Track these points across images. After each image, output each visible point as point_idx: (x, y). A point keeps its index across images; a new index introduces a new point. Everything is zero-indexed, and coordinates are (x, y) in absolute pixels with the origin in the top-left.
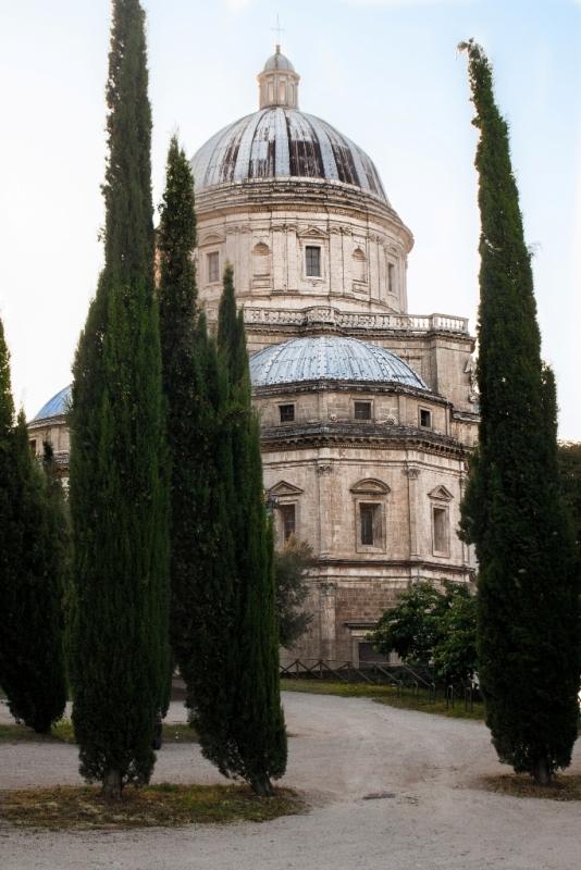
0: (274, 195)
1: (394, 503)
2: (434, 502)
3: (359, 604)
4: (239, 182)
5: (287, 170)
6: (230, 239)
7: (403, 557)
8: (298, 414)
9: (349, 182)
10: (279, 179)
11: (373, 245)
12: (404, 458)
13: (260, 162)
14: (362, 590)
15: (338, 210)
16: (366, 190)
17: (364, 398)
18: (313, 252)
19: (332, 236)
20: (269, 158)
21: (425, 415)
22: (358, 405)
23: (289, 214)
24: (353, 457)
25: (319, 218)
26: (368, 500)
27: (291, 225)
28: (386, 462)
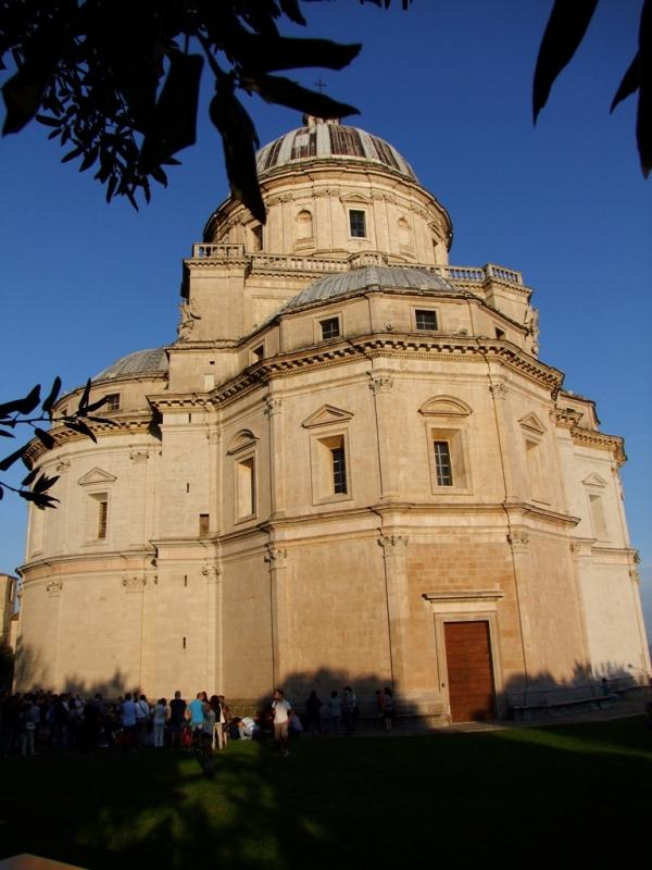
1: (477, 429)
3: (441, 567)
5: (329, 150)
7: (497, 499)
8: (346, 328)
11: (418, 217)
12: (486, 372)
13: (302, 148)
14: (443, 546)
15: (381, 179)
19: (375, 202)
21: (499, 333)
22: (418, 313)
23: (331, 182)
24: (419, 369)
25: (362, 185)
26: (442, 423)
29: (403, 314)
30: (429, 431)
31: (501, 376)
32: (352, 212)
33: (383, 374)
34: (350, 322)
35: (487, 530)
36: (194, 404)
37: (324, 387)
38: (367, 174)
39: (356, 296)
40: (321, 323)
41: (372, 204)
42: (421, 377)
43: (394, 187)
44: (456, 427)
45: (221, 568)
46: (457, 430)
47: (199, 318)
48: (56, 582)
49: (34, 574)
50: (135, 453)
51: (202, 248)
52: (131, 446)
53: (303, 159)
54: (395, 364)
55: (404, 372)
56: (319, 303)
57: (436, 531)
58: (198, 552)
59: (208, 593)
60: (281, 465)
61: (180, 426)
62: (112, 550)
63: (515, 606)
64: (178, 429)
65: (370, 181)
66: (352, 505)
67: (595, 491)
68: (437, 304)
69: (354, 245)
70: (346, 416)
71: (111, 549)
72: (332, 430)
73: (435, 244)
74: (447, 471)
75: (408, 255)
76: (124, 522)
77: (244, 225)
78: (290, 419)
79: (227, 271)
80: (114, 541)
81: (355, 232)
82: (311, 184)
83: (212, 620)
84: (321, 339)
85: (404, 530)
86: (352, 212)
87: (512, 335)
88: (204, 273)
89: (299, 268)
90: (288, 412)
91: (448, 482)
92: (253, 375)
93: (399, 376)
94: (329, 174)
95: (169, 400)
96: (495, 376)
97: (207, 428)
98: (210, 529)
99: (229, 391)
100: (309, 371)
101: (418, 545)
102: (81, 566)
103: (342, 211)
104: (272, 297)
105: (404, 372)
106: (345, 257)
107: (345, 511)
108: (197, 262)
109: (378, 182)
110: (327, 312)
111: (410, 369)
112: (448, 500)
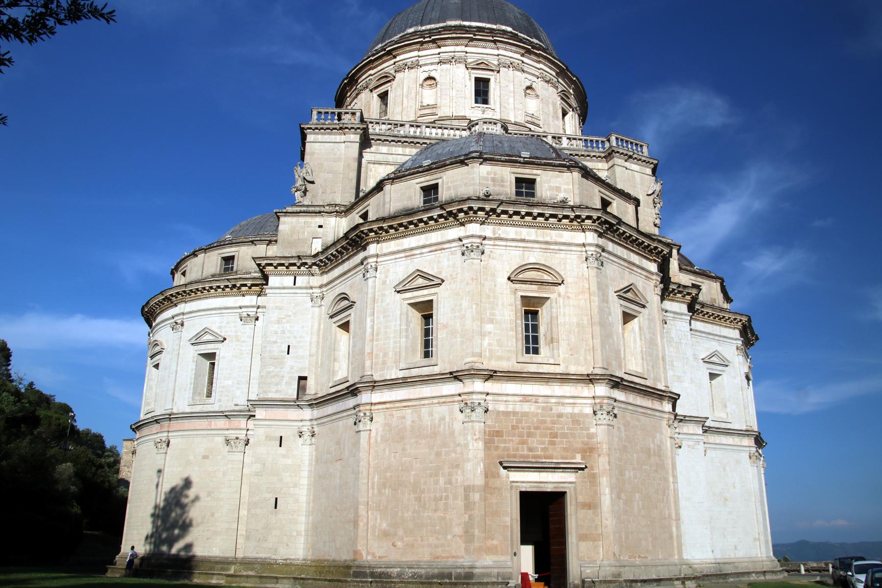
2: (622, 302)
3: (521, 435)
6: (399, 76)
8: (444, 195)
14: (525, 414)
15: (508, 47)
17: (527, 172)
21: (605, 204)
22: (519, 181)
25: (488, 52)
26: (532, 291)
27: (460, 58)
28: (556, 243)
29: (502, 181)
30: (519, 298)
31: (597, 246)
32: (478, 80)
33: (474, 240)
34: (449, 188)
35: (571, 401)
36: (299, 267)
37: (418, 252)
38: (495, 42)
39: (456, 163)
40: (422, 188)
41: (498, 72)
42: (514, 244)
43: (522, 55)
44: (545, 296)
45: (316, 429)
46: (548, 298)
47: (313, 182)
48: (164, 439)
49: (145, 431)
50: (245, 314)
51: (319, 113)
52: (240, 308)
54: (488, 230)
55: (496, 239)
56: (420, 169)
57: (517, 398)
58: (293, 413)
59: (303, 452)
61: (284, 288)
62: (217, 409)
63: (593, 478)
64: (283, 291)
65: (498, 49)
66: (436, 370)
67: (716, 369)
68: (539, 172)
69: (476, 112)
70: (437, 281)
71: (216, 408)
72: (422, 296)
73: (564, 114)
74: (536, 340)
76: (230, 382)
77: (371, 91)
78: (384, 283)
79: (343, 136)
80: (220, 401)
81: (479, 99)
82: (438, 50)
83: (305, 482)
84: (422, 204)
85: (484, 396)
86: (478, 80)
87: (618, 207)
88: (320, 137)
89: (418, 134)
90: (383, 276)
91: (536, 351)
92: (351, 239)
93: (491, 242)
94: (457, 42)
95: (275, 263)
96: (590, 245)
97: (311, 291)
98: (308, 392)
99: (332, 254)
100: (404, 236)
101: (499, 412)
102: (187, 424)
103: (467, 76)
105: (496, 239)
106: (465, 124)
107: (428, 376)
108: (313, 127)
109: (506, 50)
110: (428, 178)
111: (503, 236)
112: (533, 368)
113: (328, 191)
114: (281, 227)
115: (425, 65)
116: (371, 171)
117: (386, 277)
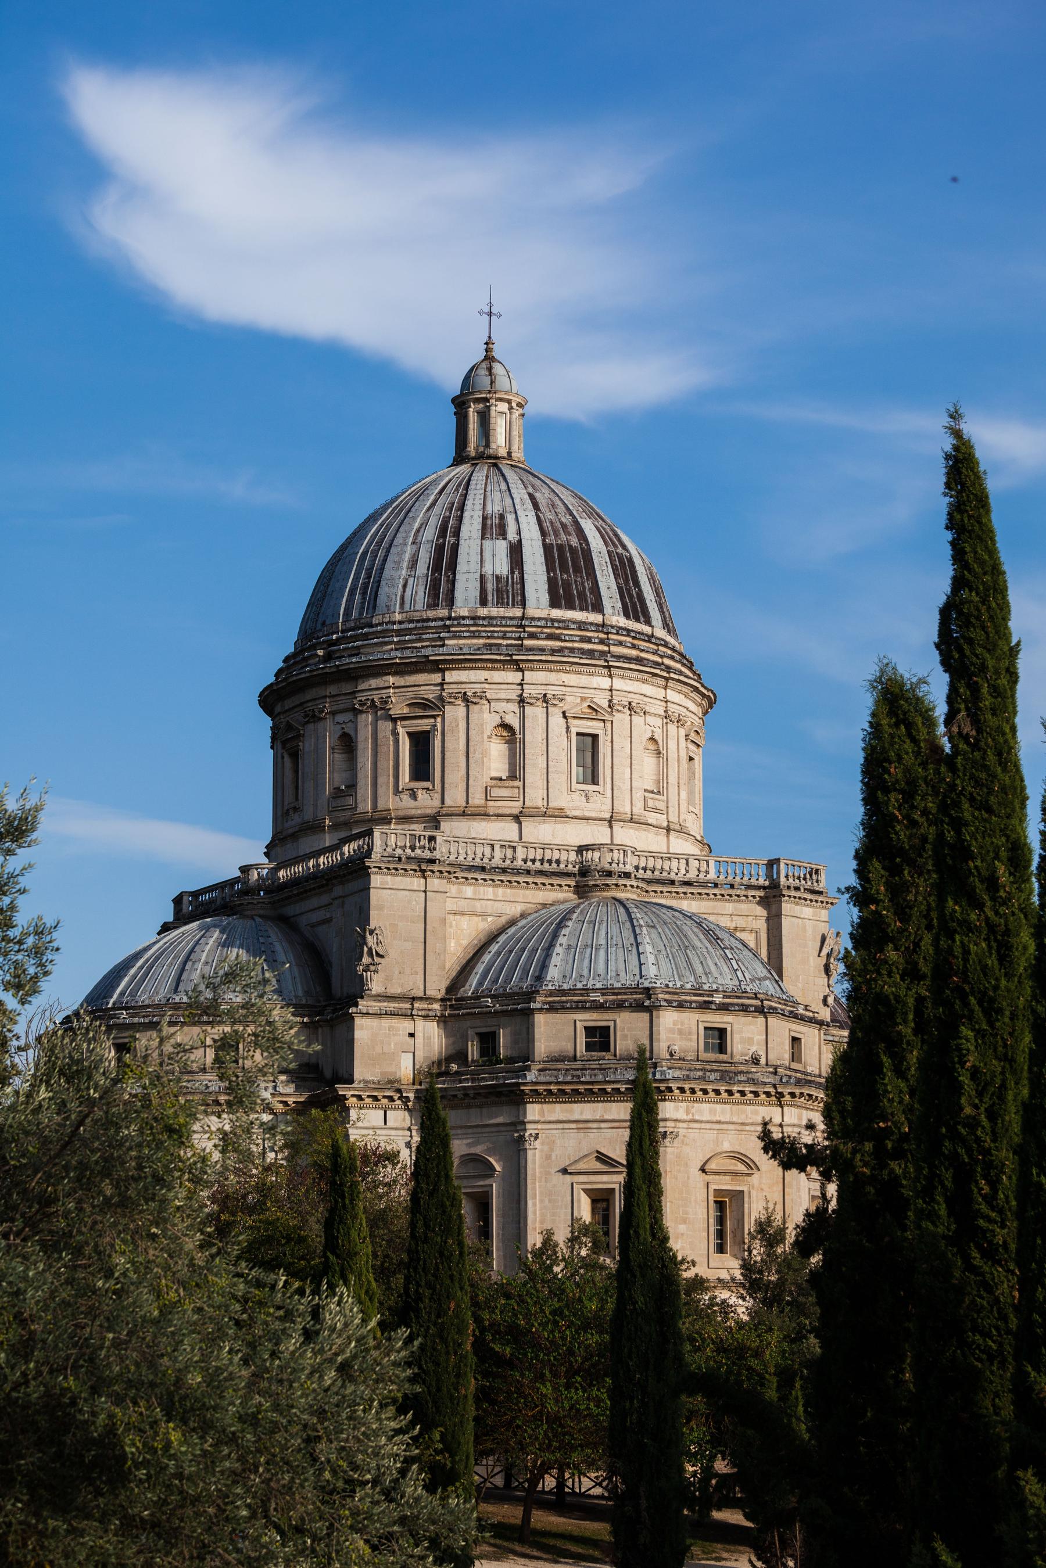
0: (526, 642)
4: (465, 612)
5: (545, 598)
9: (638, 620)
10: (531, 612)
13: (499, 578)
15: (627, 673)
16: (661, 633)
18: (590, 743)
20: (513, 573)
23: (553, 677)
25: (596, 684)
26: (726, 1184)
29: (690, 1033)
37: (595, 1125)
42: (708, 1126)
44: (738, 1188)
53: (501, 611)
55: (690, 1121)
60: (535, 1213)
75: (656, 810)
78: (548, 1157)
88: (389, 880)
90: (546, 1148)
93: (685, 1125)
104: (473, 914)
105: (690, 1121)
109: (623, 677)
111: (697, 1117)
113: (407, 971)
114: (358, 1034)
115: (498, 700)
116: (451, 926)
117: (552, 1150)
